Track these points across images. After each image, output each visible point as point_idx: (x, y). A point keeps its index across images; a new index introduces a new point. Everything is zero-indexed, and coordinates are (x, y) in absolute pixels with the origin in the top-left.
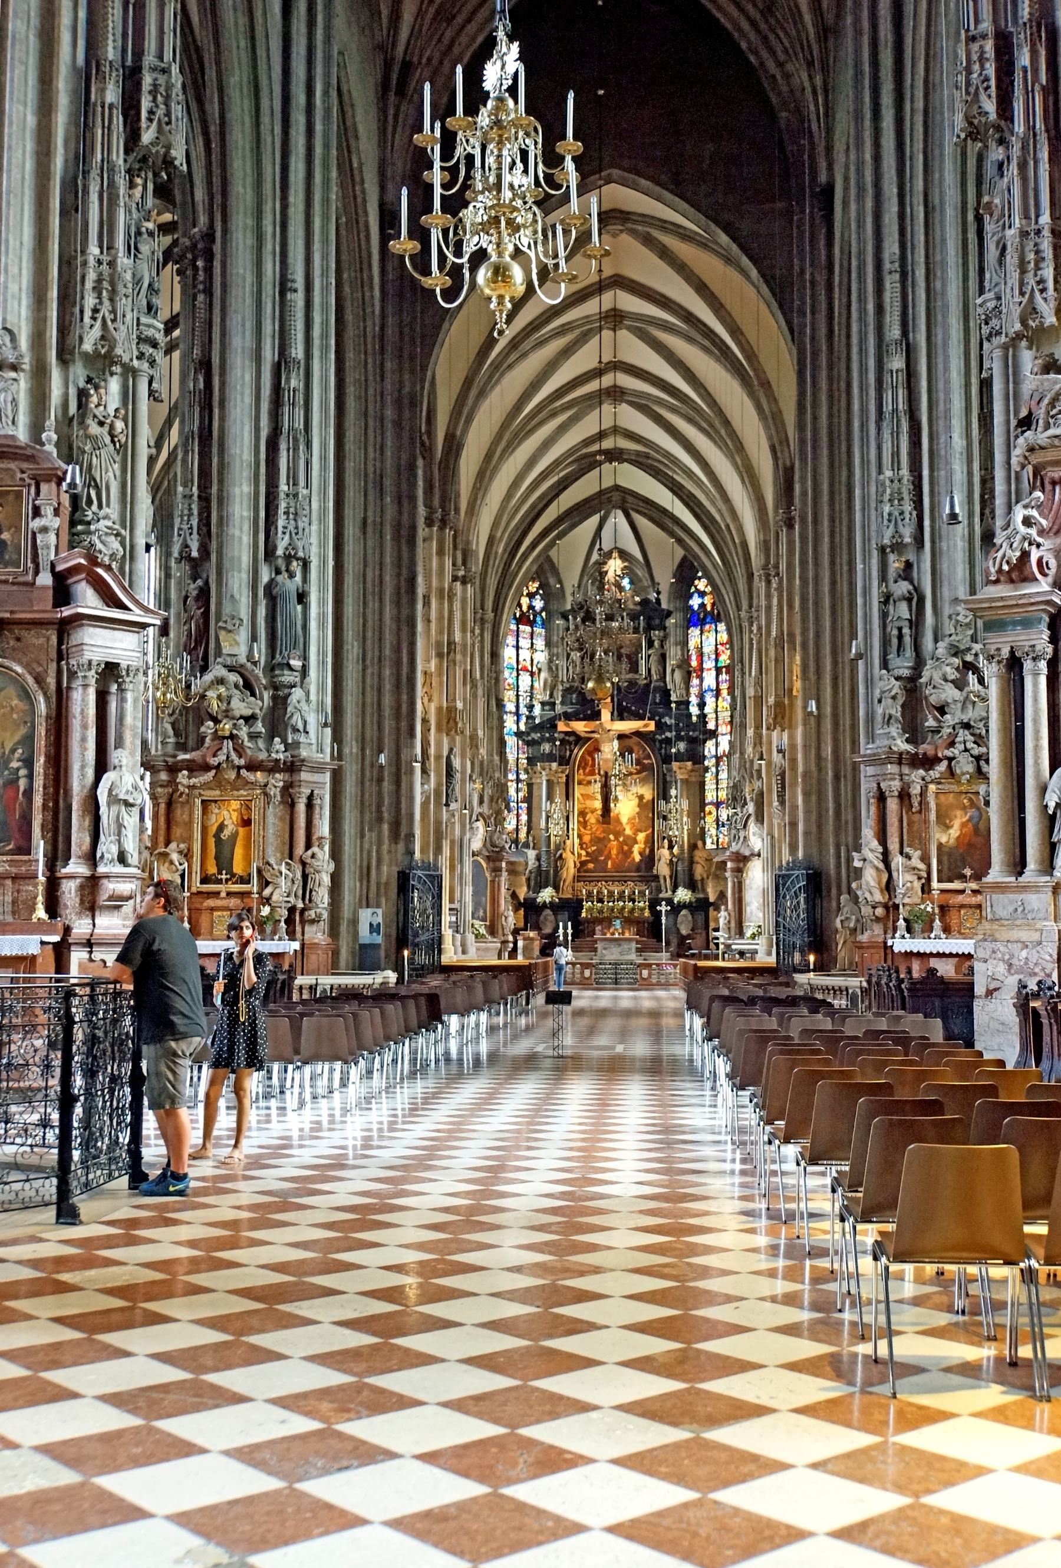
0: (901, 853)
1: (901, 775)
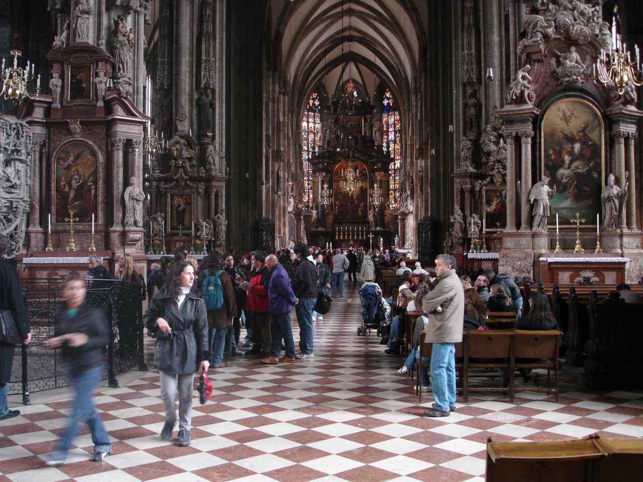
0: (471, 216)
1: (471, 182)
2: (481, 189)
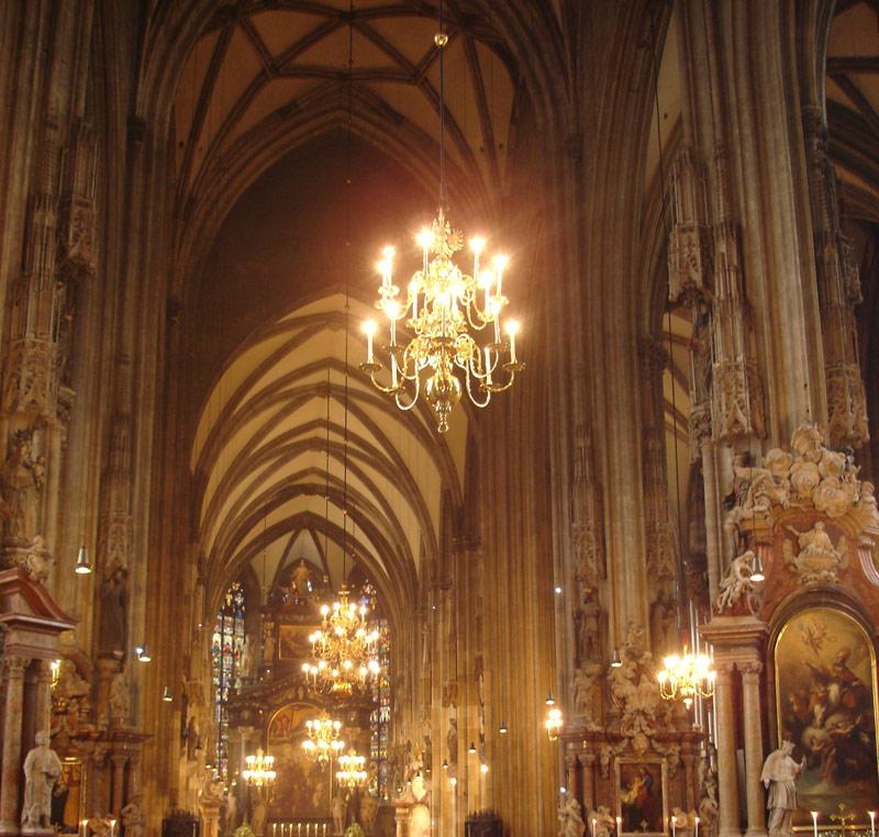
0: (595, 810)
2: (610, 764)
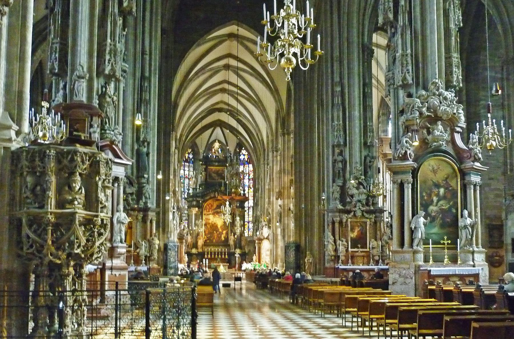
2: (347, 221)
